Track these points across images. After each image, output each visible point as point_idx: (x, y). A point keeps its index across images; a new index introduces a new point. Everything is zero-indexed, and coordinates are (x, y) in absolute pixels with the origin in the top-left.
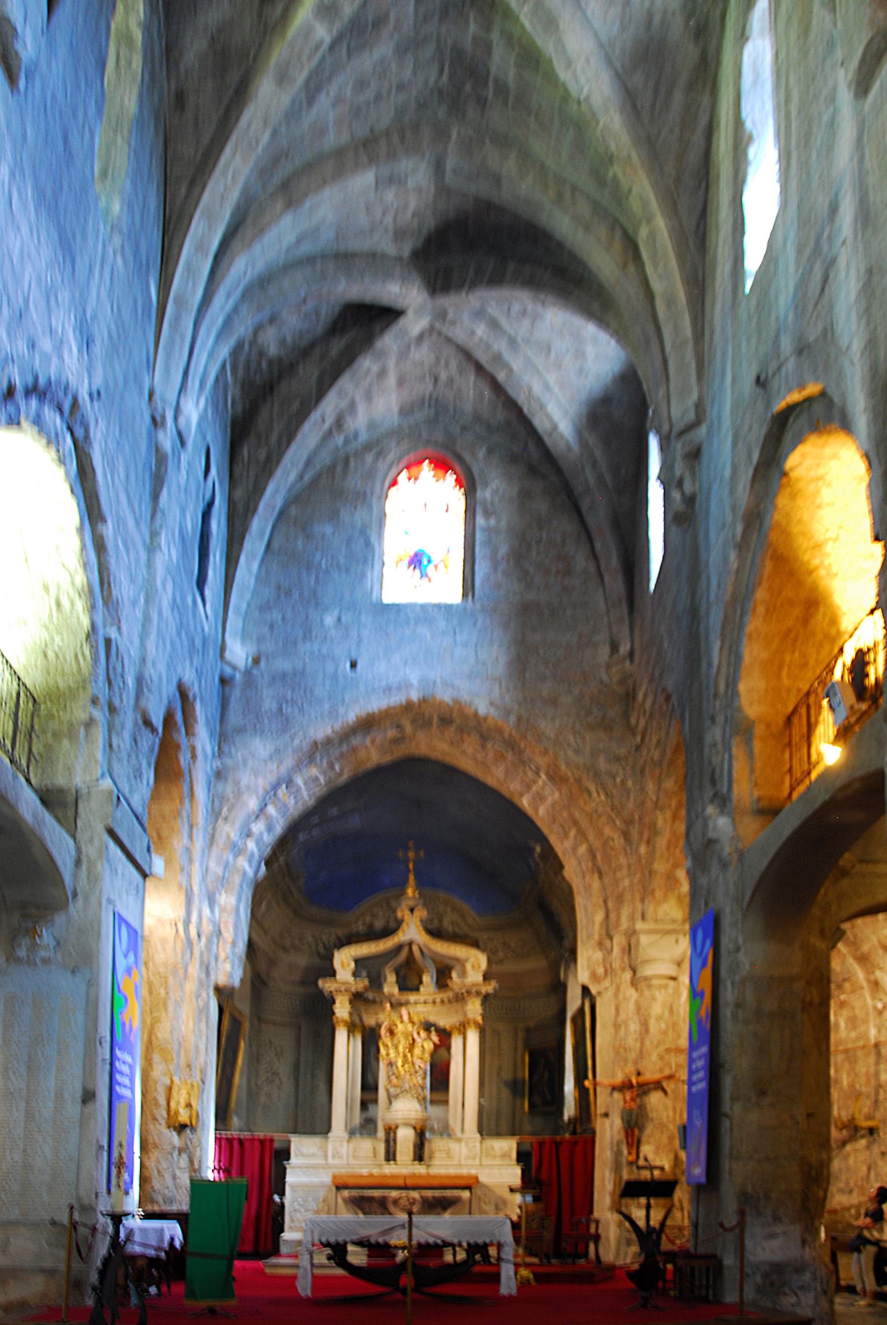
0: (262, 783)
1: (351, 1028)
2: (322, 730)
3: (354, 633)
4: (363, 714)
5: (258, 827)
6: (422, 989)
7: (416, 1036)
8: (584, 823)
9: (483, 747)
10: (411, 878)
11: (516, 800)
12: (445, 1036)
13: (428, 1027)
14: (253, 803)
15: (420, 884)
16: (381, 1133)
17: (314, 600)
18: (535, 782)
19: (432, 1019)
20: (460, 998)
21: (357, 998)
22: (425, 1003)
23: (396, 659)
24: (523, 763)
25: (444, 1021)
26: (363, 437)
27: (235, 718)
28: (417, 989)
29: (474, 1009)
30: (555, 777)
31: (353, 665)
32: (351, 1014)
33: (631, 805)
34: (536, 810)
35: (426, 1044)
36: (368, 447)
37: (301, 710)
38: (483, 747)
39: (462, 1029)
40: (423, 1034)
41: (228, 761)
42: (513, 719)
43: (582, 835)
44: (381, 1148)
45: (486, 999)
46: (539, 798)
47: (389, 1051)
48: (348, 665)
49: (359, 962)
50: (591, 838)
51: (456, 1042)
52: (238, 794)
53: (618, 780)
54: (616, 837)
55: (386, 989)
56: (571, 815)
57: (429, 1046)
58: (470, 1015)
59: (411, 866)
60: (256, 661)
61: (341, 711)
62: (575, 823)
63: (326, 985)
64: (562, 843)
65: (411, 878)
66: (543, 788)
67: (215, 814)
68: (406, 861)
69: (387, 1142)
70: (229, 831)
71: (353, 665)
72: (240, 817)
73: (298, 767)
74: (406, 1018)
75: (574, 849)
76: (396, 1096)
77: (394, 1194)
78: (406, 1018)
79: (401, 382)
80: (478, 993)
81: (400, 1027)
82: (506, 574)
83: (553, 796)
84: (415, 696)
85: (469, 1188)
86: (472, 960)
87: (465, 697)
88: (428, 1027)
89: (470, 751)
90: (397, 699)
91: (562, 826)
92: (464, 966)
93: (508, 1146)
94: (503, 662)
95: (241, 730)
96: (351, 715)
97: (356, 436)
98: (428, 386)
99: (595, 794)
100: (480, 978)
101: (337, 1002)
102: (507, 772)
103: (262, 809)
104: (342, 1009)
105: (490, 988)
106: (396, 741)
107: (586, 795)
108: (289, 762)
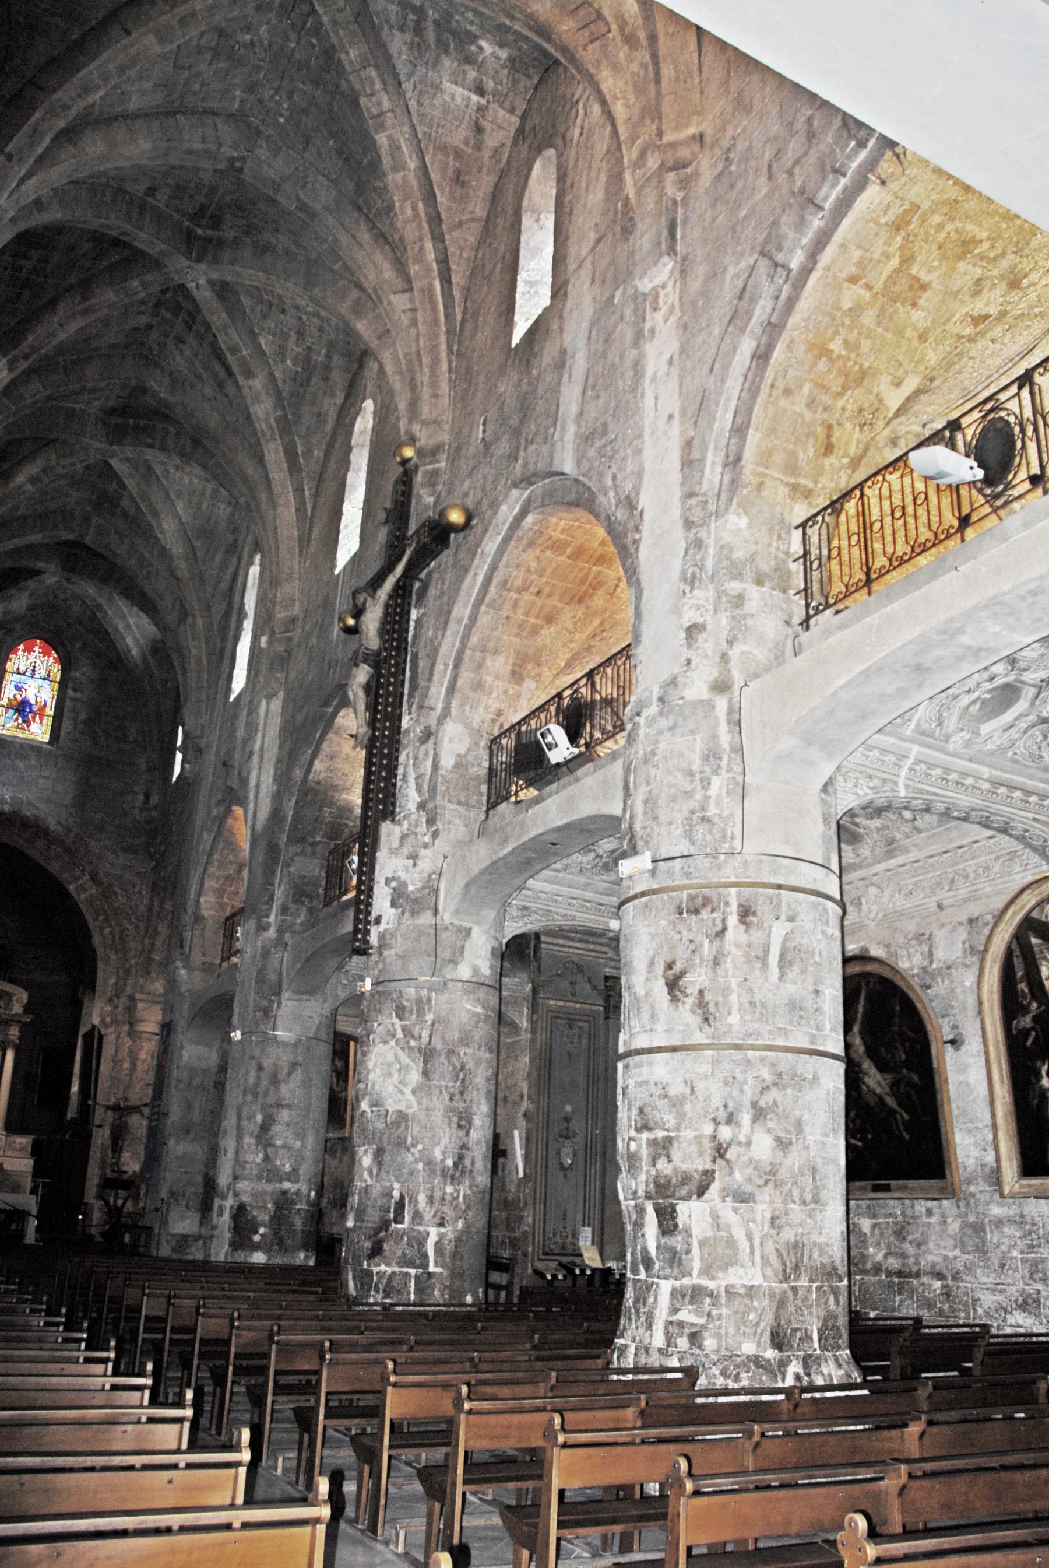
45: (24, 1026)
58: (11, 1038)
75: (102, 929)
87: (42, 815)
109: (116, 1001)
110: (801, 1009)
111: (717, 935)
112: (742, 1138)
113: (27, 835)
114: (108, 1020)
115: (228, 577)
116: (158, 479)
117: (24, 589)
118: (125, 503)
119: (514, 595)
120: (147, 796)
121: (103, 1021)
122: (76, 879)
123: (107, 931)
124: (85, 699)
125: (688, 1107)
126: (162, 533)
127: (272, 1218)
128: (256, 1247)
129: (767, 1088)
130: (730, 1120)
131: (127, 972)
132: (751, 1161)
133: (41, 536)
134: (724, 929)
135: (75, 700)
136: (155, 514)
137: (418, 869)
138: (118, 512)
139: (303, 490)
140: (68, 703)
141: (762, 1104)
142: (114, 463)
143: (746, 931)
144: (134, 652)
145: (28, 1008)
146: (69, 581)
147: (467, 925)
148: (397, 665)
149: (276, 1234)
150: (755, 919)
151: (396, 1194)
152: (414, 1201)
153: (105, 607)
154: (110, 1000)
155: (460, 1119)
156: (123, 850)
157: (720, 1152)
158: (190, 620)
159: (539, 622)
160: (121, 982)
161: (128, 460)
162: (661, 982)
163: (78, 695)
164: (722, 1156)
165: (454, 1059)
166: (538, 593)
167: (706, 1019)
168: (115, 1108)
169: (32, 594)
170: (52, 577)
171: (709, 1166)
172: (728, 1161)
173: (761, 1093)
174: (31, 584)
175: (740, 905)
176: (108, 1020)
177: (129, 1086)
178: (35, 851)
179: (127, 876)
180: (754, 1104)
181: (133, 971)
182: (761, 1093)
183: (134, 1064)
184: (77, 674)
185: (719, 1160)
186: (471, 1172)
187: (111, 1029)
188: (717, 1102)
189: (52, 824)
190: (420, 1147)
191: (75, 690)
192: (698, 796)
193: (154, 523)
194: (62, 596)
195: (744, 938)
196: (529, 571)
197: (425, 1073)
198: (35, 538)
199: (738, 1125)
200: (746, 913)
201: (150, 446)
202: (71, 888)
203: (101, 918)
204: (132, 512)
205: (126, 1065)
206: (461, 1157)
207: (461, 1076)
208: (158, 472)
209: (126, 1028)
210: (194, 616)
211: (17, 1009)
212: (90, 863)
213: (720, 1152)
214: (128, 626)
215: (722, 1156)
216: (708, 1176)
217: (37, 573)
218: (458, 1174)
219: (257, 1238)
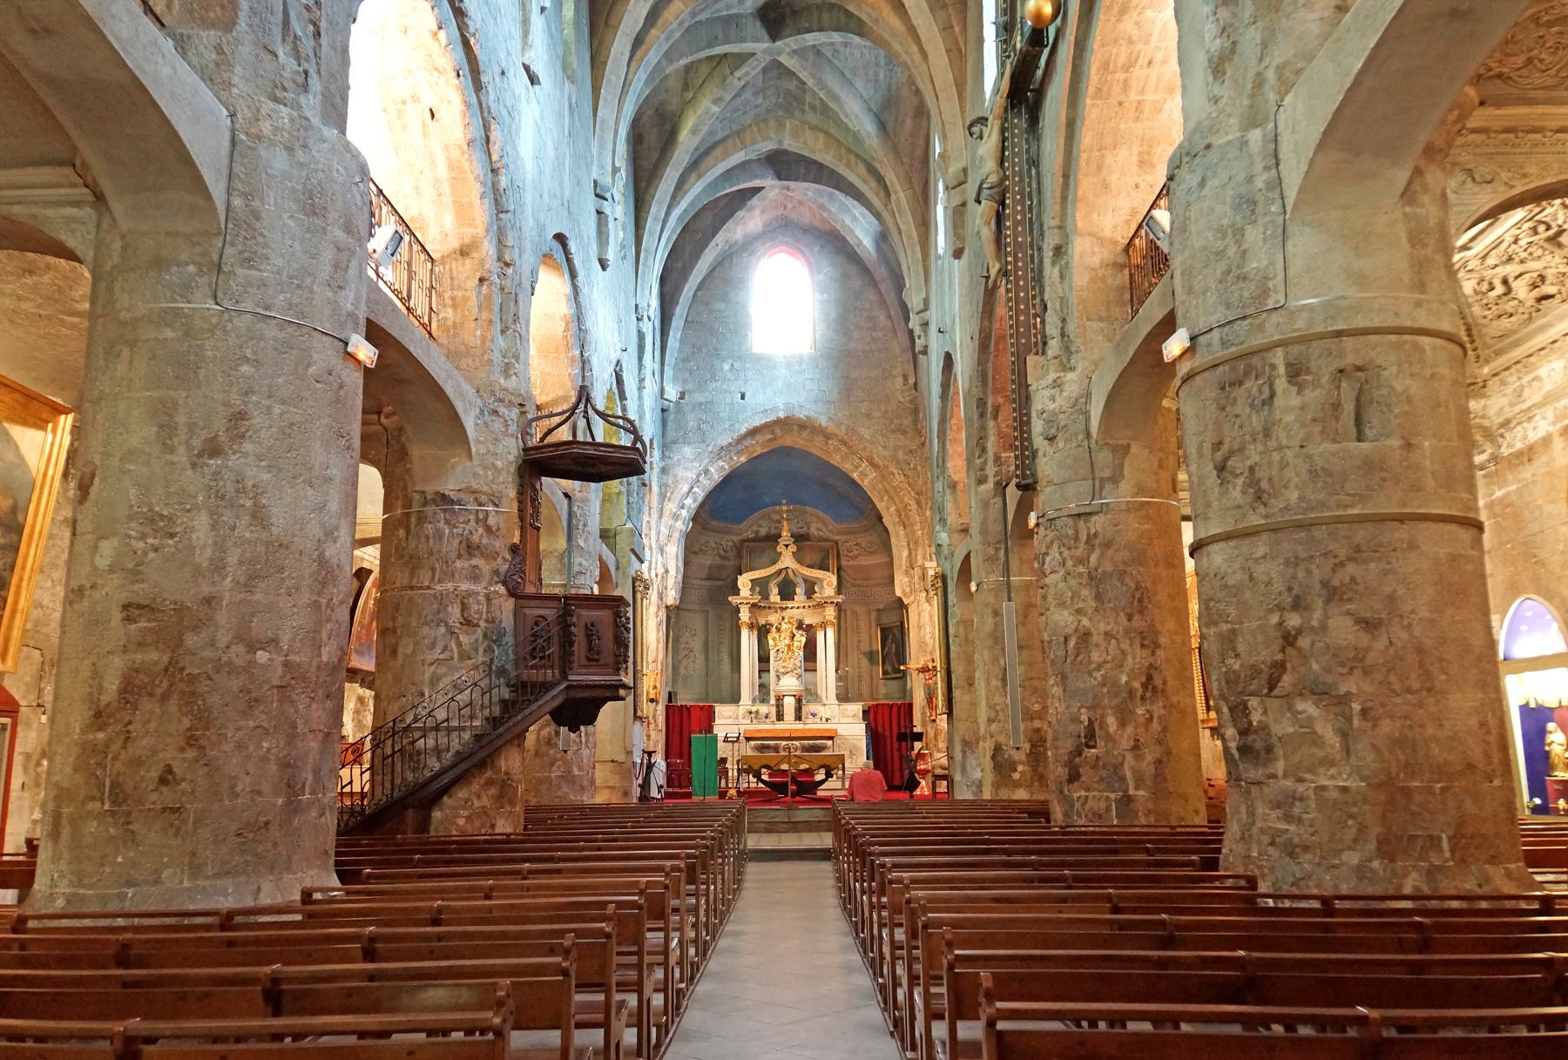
0: (692, 475)
1: (751, 626)
2: (725, 440)
3: (742, 374)
8: (892, 493)
12: (810, 630)
13: (800, 626)
14: (685, 489)
16: (773, 701)
17: (716, 354)
20: (821, 606)
23: (769, 392)
24: (853, 453)
26: (741, 242)
27: (671, 434)
29: (830, 613)
30: (871, 463)
31: (743, 397)
35: (801, 639)
39: (824, 625)
41: (669, 461)
42: (843, 428)
43: (891, 498)
44: (773, 711)
46: (863, 474)
47: (776, 642)
52: (676, 482)
60: (682, 397)
61: (737, 426)
62: (887, 492)
63: (733, 600)
67: (663, 496)
69: (778, 706)
70: (671, 507)
71: (743, 397)
72: (677, 497)
73: (711, 462)
75: (888, 509)
77: (784, 743)
81: (784, 626)
82: (836, 331)
83: (873, 475)
84: (782, 415)
85: (831, 738)
87: (813, 415)
90: (771, 418)
93: (856, 708)
94: (835, 392)
95: (675, 442)
96: (743, 430)
97: (736, 243)
98: (780, 212)
102: (842, 458)
104: (745, 615)
105: (839, 599)
110: (1382, 469)
111: (1264, 403)
112: (1315, 623)
113: (805, 434)
115: (921, 142)
116: (830, 62)
117: (752, 209)
118: (808, 98)
119: (1120, 76)
120: (906, 378)
122: (857, 467)
123: (893, 509)
125: (1248, 595)
126: (847, 116)
127: (1028, 755)
128: (1017, 785)
129: (1342, 564)
130: (1297, 605)
131: (916, 542)
132: (1328, 647)
133: (742, 153)
134: (1273, 395)
136: (836, 99)
137: (1064, 394)
138: (807, 107)
139: (952, 27)
141: (1335, 582)
142: (783, 59)
143: (1298, 393)
144: (865, 242)
145: (839, 591)
146: (788, 189)
147: (1125, 442)
148: (1021, 193)
149: (1034, 771)
150: (1309, 378)
151: (1084, 718)
152: (1103, 725)
153: (828, 206)
155: (1143, 638)
156: (893, 431)
157: (1289, 639)
158: (893, 197)
159: (1159, 96)
161: (795, 52)
162: (1211, 466)
164: (1291, 645)
165: (1127, 580)
166: (1150, 63)
167: (1259, 498)
168: (924, 670)
169: (763, 212)
170: (771, 185)
171: (1279, 657)
172: (1299, 650)
173: (1334, 571)
174: (755, 201)
175: (1288, 365)
176: (908, 590)
178: (816, 448)
179: (901, 455)
180: (1325, 584)
182: (1334, 571)
185: (1289, 650)
186: (1163, 691)
187: (912, 598)
188: (1278, 585)
189: (824, 422)
190: (1103, 672)
192: (1232, 251)
193: (837, 109)
194: (790, 206)
195: (1295, 401)
196: (1131, 42)
197: (1098, 597)
198: (738, 158)
199: (1308, 608)
200: (1296, 372)
201: (809, 31)
202: (855, 476)
204: (817, 103)
206: (1150, 678)
207: (1138, 595)
208: (829, 55)
209: (924, 595)
210: (896, 192)
212: (865, 449)
213: (1289, 639)
214: (855, 219)
215: (1291, 645)
216: (1279, 667)
217: (759, 189)
218: (1148, 695)
219: (1016, 776)
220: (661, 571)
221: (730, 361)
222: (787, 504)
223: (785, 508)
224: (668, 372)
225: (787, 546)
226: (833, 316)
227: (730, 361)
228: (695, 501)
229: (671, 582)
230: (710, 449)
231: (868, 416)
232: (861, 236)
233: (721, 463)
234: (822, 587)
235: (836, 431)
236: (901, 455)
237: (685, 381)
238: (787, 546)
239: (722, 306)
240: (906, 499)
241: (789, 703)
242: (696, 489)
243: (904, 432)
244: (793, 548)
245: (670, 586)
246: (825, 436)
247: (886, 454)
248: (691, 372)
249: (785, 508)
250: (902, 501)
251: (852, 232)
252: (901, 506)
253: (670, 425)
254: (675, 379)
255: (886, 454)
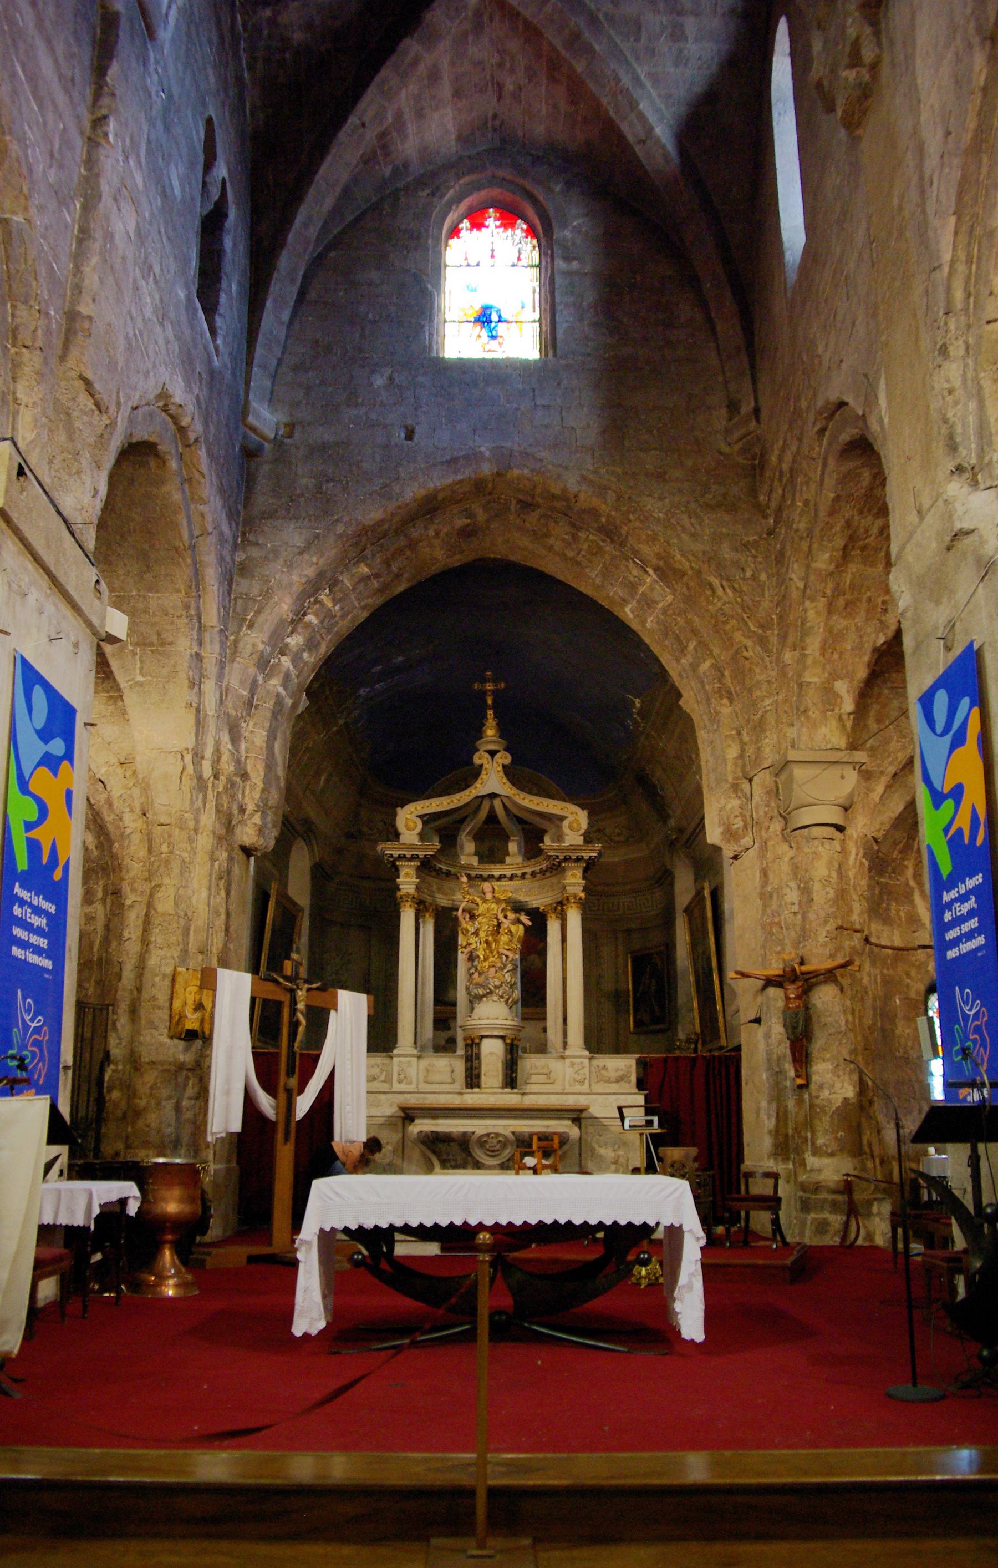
2: (374, 514)
4: (423, 492)
5: (295, 641)
6: (508, 859)
7: (501, 917)
9: (574, 537)
10: (490, 713)
11: (616, 611)
12: (538, 920)
15: (503, 732)
18: (642, 582)
19: (521, 897)
20: (556, 868)
21: (426, 866)
22: (512, 878)
25: (538, 899)
27: (262, 501)
28: (502, 862)
29: (574, 880)
30: (667, 573)
31: (410, 435)
32: (418, 888)
33: (766, 604)
34: (643, 622)
36: (421, 182)
37: (344, 489)
38: (574, 537)
39: (560, 908)
40: (511, 916)
41: (255, 552)
42: (611, 496)
45: (589, 867)
48: (403, 435)
49: (427, 819)
50: (716, 651)
51: (553, 927)
52: (267, 594)
53: (749, 574)
54: (749, 643)
55: (463, 860)
56: (689, 622)
57: (519, 931)
58: (570, 889)
59: (490, 701)
61: (396, 488)
62: (695, 632)
63: (390, 850)
64: (678, 661)
65: (490, 713)
66: (652, 589)
68: (483, 694)
71: (410, 435)
74: (489, 896)
75: (694, 667)
76: (480, 998)
78: (489, 896)
79: (457, 94)
80: (578, 859)
81: (482, 908)
83: (665, 597)
86: (571, 818)
88: (518, 907)
89: (558, 546)
91: (677, 638)
92: (559, 827)
95: (270, 515)
96: (412, 492)
99: (720, 592)
100: (580, 841)
101: (402, 873)
103: (300, 614)
104: (408, 882)
106: (467, 533)
107: (708, 593)
108: (331, 551)
109: (746, 786)
113: (533, 519)
114: (738, 824)
120: (733, 407)
121: (730, 834)
123: (705, 666)
124: (588, 269)
135: (568, 274)
140: (559, 281)
144: (658, 130)
154: (735, 787)
156: (709, 507)
160: (750, 750)
163: (575, 265)
177: (804, 935)
179: (726, 552)
181: (771, 719)
183: (806, 890)
184: (568, 234)
187: (747, 841)
191: (567, 259)
202: (628, 613)
203: (692, 645)
205: (792, 895)
209: (777, 826)
211: (573, 838)
214: (637, 79)
220: (227, 767)
221: (388, 371)
222: (495, 681)
223: (489, 687)
224: (260, 380)
225: (492, 753)
226: (590, 297)
227: (388, 371)
228: (311, 645)
229: (251, 796)
230: (340, 529)
231: (661, 476)
232: (652, 118)
233: (364, 570)
234: (559, 838)
235: (596, 502)
236: (726, 552)
237: (295, 405)
238: (492, 753)
239: (374, 275)
240: (738, 636)
241: (492, 1051)
242: (311, 618)
243: (732, 509)
244: (505, 758)
245: (250, 807)
246: (573, 525)
247: (697, 547)
248: (309, 389)
249: (489, 687)
250: (728, 642)
251: (633, 105)
252: (725, 657)
253: (262, 484)
254: (272, 399)
255: (697, 547)
